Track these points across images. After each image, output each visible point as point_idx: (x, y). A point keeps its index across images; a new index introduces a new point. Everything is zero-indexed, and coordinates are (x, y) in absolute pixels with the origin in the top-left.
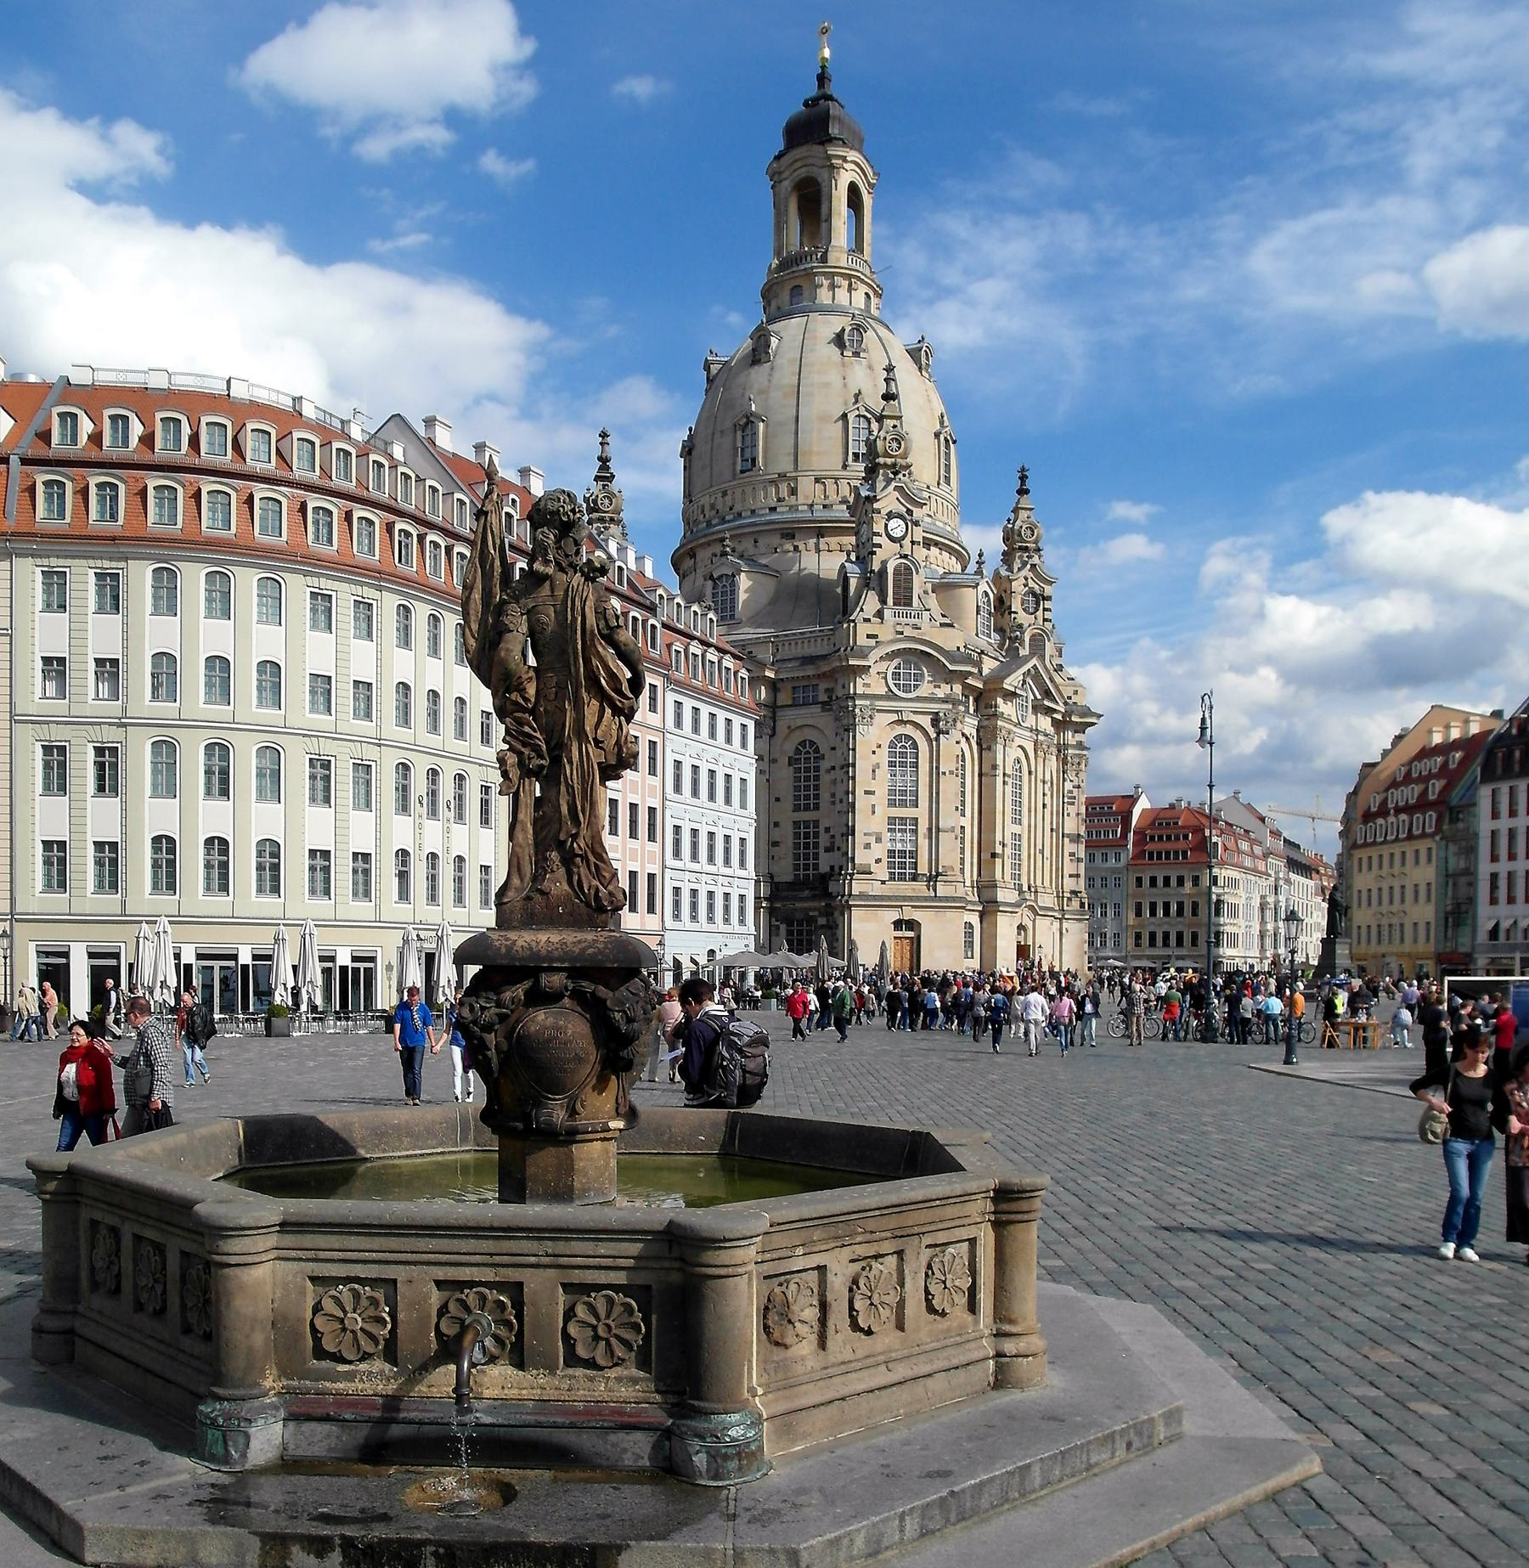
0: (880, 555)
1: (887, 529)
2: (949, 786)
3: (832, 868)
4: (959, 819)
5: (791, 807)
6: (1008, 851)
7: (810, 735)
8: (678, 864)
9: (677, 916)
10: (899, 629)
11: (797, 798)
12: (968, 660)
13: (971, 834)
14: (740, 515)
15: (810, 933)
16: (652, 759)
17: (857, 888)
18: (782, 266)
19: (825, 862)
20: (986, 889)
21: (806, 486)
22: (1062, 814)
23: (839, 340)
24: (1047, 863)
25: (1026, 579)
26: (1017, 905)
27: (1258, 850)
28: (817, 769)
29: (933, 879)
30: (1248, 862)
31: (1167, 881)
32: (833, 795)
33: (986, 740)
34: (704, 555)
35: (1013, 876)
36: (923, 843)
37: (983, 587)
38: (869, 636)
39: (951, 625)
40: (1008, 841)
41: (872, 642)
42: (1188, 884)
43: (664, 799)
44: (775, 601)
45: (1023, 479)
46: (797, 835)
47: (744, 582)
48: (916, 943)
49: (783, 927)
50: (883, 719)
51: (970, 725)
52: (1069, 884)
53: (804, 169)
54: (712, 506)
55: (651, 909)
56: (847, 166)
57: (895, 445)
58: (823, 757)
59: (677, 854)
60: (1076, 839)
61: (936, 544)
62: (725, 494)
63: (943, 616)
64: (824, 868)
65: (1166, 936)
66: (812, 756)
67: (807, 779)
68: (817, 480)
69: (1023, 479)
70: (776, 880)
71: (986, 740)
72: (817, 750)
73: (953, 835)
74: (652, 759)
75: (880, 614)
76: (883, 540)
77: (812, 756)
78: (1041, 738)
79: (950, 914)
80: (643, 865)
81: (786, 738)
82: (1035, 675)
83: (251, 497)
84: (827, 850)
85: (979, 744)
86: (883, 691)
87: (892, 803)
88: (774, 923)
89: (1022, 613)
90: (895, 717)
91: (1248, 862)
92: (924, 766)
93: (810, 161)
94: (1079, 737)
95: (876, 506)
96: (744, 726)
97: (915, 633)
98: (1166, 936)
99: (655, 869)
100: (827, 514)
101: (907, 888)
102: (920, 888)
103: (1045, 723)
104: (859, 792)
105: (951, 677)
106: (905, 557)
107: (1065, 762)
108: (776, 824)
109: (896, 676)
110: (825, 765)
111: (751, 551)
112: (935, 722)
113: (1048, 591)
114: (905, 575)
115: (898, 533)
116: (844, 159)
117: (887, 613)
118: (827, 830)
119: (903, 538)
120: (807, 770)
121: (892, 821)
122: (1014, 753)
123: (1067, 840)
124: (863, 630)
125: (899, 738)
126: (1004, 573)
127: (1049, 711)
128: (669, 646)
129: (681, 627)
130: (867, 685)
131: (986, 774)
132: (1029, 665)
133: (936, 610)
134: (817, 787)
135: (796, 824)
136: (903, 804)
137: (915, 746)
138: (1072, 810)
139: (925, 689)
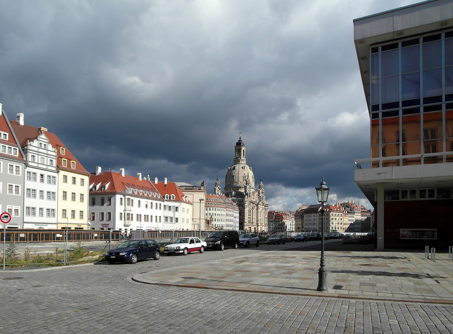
1: (248, 190)
4: (255, 217)
13: (256, 218)
20: (257, 224)
21: (239, 183)
23: (242, 168)
27: (290, 217)
29: (252, 223)
31: (278, 222)
33: (257, 209)
36: (251, 220)
37: (257, 193)
42: (281, 222)
44: (236, 195)
47: (233, 193)
48: (251, 229)
51: (256, 208)
52: (266, 223)
64: (242, 222)
65: (278, 228)
71: (257, 209)
75: (247, 198)
82: (262, 202)
87: (248, 216)
91: (288, 219)
92: (251, 212)
94: (267, 207)
97: (251, 200)
98: (278, 228)
100: (241, 186)
102: (251, 224)
103: (263, 207)
104: (245, 215)
109: (249, 204)
112: (253, 208)
113: (264, 192)
115: (249, 190)
117: (248, 198)
121: (248, 217)
124: (246, 199)
126: (259, 190)
127: (264, 205)
131: (257, 212)
136: (249, 216)
138: (266, 215)
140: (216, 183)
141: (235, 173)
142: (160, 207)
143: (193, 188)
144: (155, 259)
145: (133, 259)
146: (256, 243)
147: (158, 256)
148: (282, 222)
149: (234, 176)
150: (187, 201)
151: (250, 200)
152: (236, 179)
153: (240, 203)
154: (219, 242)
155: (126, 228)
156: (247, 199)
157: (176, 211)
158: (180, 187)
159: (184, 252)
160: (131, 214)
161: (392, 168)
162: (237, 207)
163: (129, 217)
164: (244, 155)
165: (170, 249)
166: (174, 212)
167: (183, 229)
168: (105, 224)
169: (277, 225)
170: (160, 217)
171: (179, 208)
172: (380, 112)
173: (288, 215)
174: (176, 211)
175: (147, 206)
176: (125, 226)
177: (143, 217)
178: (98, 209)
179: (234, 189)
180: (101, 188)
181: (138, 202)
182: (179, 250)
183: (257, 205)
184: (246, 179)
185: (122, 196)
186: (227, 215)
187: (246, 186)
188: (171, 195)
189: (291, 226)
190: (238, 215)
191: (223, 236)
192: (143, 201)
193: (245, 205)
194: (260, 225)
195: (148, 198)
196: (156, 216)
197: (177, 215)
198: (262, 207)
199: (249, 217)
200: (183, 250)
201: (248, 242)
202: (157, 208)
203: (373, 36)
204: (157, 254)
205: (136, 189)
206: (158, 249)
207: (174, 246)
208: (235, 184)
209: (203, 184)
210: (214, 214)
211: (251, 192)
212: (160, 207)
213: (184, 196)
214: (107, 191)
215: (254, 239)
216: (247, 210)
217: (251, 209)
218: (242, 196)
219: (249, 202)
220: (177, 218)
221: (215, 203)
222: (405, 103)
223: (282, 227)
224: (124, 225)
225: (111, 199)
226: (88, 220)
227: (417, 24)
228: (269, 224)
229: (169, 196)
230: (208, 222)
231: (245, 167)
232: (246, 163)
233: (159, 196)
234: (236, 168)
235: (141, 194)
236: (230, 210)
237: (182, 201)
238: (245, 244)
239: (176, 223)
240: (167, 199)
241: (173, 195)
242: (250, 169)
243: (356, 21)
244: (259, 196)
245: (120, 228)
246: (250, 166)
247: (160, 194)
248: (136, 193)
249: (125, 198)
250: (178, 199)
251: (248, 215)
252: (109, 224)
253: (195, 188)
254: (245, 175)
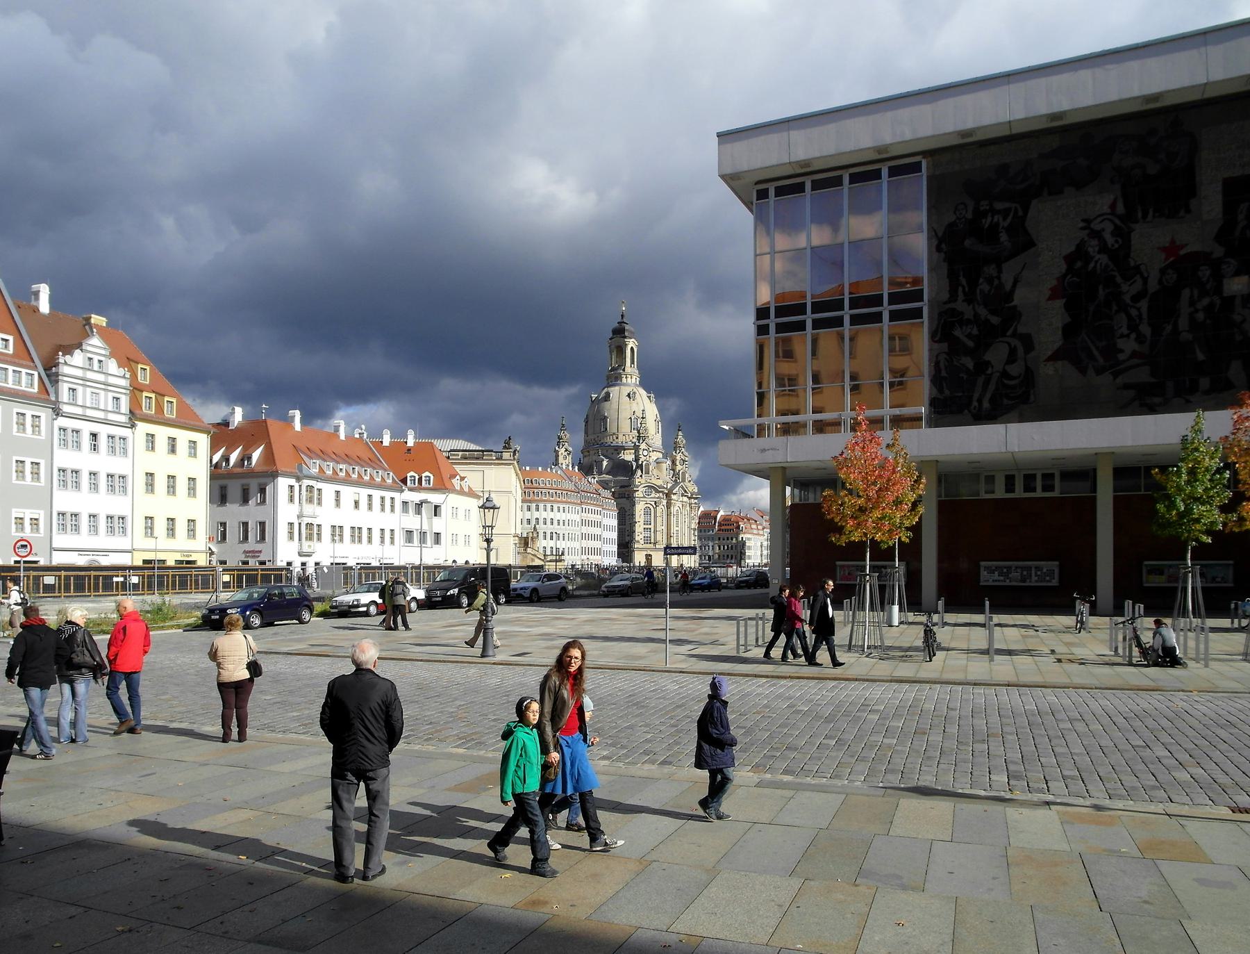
0: (641, 460)
2: (659, 520)
4: (661, 527)
13: (665, 531)
18: (611, 371)
19: (627, 539)
21: (620, 436)
22: (690, 523)
23: (629, 395)
24: (686, 537)
29: (655, 544)
31: (728, 539)
33: (669, 506)
36: (652, 534)
37: (668, 462)
40: (675, 532)
44: (612, 468)
47: (605, 463)
51: (664, 502)
60: (694, 530)
65: (728, 556)
71: (669, 506)
75: (641, 476)
82: (682, 487)
91: (755, 532)
97: (650, 481)
98: (728, 556)
103: (685, 499)
105: (660, 492)
109: (645, 492)
110: (627, 514)
112: (655, 504)
113: (687, 459)
115: (645, 454)
122: (676, 508)
124: (637, 480)
127: (686, 496)
131: (669, 515)
136: (647, 524)
140: (560, 438)
141: (609, 409)
142: (392, 507)
143: (483, 455)
144: (301, 622)
145: (253, 622)
146: (558, 593)
147: (306, 615)
148: (737, 539)
149: (605, 418)
150: (466, 490)
151: (649, 483)
152: (611, 428)
153: (623, 489)
154: (456, 590)
155: (304, 559)
156: (640, 480)
157: (435, 515)
158: (449, 452)
159: (368, 609)
160: (315, 525)
161: (785, 440)
162: (613, 501)
163: (312, 531)
164: (632, 362)
165: (341, 605)
166: (430, 519)
167: (454, 561)
168: (253, 552)
169: (726, 547)
170: (392, 531)
171: (443, 508)
172: (772, 322)
173: (756, 521)
174: (435, 515)
175: (357, 503)
176: (301, 554)
177: (347, 533)
178: (234, 513)
179: (605, 453)
180: (242, 460)
181: (333, 495)
182: (358, 606)
184: (639, 425)
185: (292, 481)
186: (584, 523)
187: (637, 444)
188: (424, 475)
189: (762, 551)
190: (614, 522)
191: (465, 578)
192: (348, 493)
193: (636, 494)
195: (359, 483)
196: (382, 530)
197: (438, 525)
198: (681, 499)
199: (647, 529)
200: (368, 605)
201: (535, 590)
202: (383, 510)
203: (753, 168)
204: (304, 613)
205: (328, 463)
206: (306, 603)
207: (349, 599)
208: (609, 440)
209: (509, 445)
210: (541, 521)
211: (651, 461)
212: (392, 507)
213: (458, 477)
214: (260, 469)
215: (551, 584)
216: (639, 508)
217: (651, 507)
218: (625, 471)
219: (645, 487)
220: (438, 534)
221: (551, 491)
222: (817, 307)
223: (737, 553)
224: (299, 553)
225: (265, 489)
226: (208, 540)
227: (832, 151)
228: (705, 547)
229: (417, 477)
230: (525, 542)
231: (634, 393)
232: (638, 383)
233: (388, 478)
234: (611, 395)
235: (342, 474)
236: (593, 508)
237: (454, 491)
238: (527, 594)
239: (434, 546)
240: (413, 485)
241: (427, 474)
242: (650, 399)
243: (723, 136)
244: (673, 470)
245: (290, 560)
246: (648, 392)
247: (391, 474)
248: (329, 472)
249: (300, 486)
250: (442, 486)
251: (642, 522)
252: (260, 552)
253: (487, 455)
254: (636, 414)
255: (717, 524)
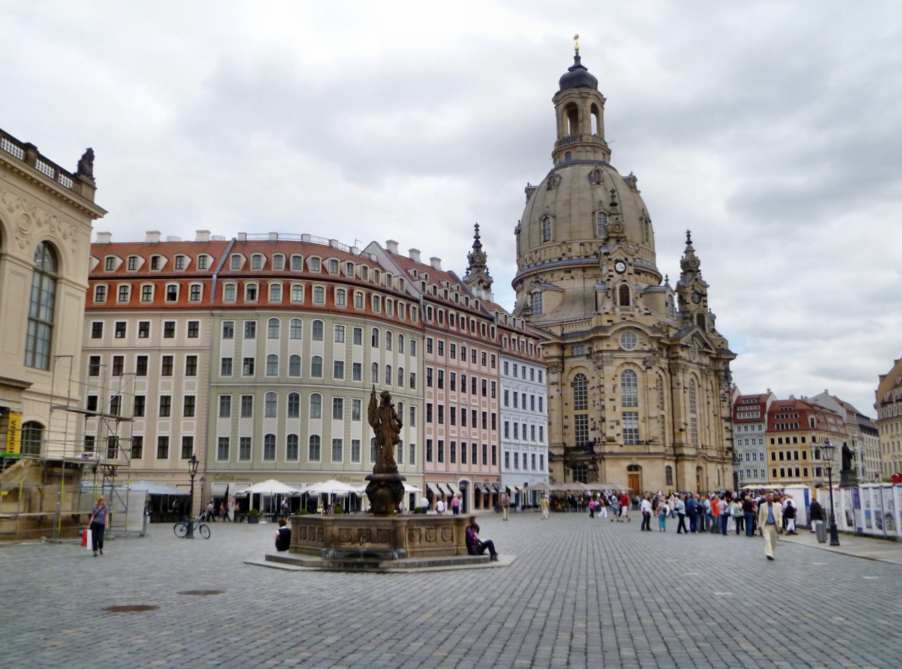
3: (595, 439)
5: (573, 408)
6: (689, 427)
7: (581, 371)
8: (507, 441)
9: (507, 466)
10: (623, 317)
11: (576, 403)
12: (660, 330)
13: (668, 418)
14: (544, 262)
15: (585, 473)
16: (494, 390)
17: (607, 449)
21: (576, 247)
25: (693, 286)
26: (696, 456)
27: (840, 422)
28: (586, 388)
30: (834, 429)
32: (594, 401)
33: (672, 371)
34: (527, 282)
35: (693, 441)
38: (609, 321)
39: (649, 314)
41: (610, 324)
43: (499, 409)
45: (689, 236)
46: (577, 422)
49: (571, 471)
50: (619, 362)
51: (664, 363)
53: (569, 99)
54: (531, 258)
55: (494, 463)
56: (589, 96)
57: (617, 227)
58: (588, 382)
59: (507, 435)
61: (644, 272)
62: (536, 252)
63: (646, 309)
64: (591, 439)
66: (583, 381)
67: (581, 393)
68: (581, 244)
69: (689, 236)
70: (567, 446)
72: (585, 379)
73: (656, 421)
74: (494, 390)
75: (613, 309)
76: (614, 273)
77: (583, 381)
78: (704, 368)
79: (659, 462)
80: (489, 442)
81: (570, 372)
83: (311, 287)
84: (593, 429)
85: (670, 372)
86: (616, 348)
87: (624, 405)
88: (567, 468)
89: (692, 303)
90: (622, 361)
93: (572, 95)
95: (610, 257)
96: (540, 372)
97: (632, 319)
99: (495, 443)
100: (587, 260)
101: (634, 449)
102: (641, 449)
103: (706, 360)
104: (607, 400)
106: (625, 281)
107: (720, 380)
108: (566, 417)
109: (623, 341)
110: (589, 386)
111: (550, 280)
112: (644, 363)
114: (625, 291)
115: (621, 270)
116: (589, 94)
118: (592, 419)
119: (623, 272)
120: (581, 389)
121: (624, 414)
123: (723, 420)
125: (626, 371)
127: (707, 353)
128: (500, 336)
129: (507, 326)
130: (608, 345)
132: (694, 331)
133: (642, 307)
134: (586, 398)
135: (576, 417)
136: (630, 405)
137: (635, 375)
139: (638, 346)
183: (669, 348)
194: (692, 452)
198: (697, 360)
199: (630, 413)
217: (636, 370)
251: (619, 400)
255: (766, 416)
